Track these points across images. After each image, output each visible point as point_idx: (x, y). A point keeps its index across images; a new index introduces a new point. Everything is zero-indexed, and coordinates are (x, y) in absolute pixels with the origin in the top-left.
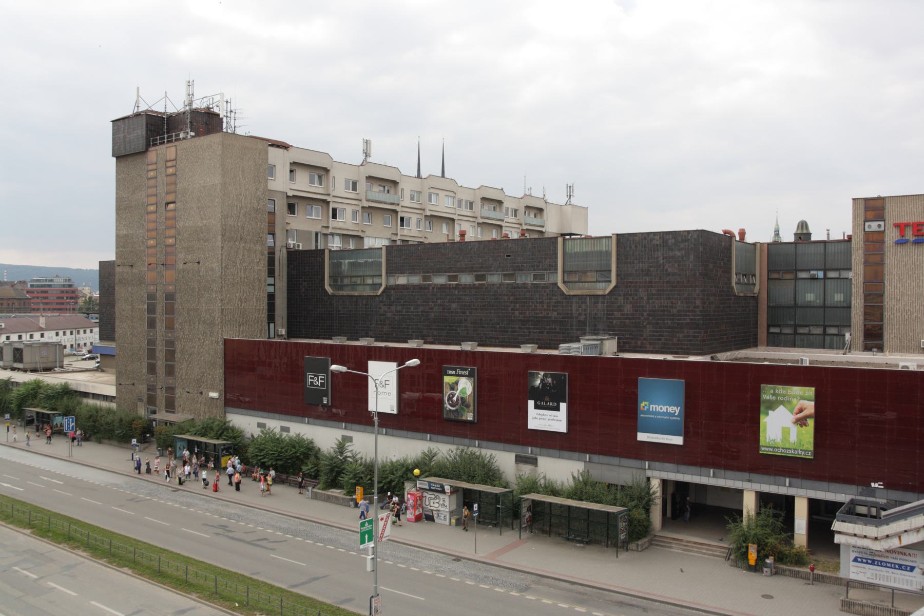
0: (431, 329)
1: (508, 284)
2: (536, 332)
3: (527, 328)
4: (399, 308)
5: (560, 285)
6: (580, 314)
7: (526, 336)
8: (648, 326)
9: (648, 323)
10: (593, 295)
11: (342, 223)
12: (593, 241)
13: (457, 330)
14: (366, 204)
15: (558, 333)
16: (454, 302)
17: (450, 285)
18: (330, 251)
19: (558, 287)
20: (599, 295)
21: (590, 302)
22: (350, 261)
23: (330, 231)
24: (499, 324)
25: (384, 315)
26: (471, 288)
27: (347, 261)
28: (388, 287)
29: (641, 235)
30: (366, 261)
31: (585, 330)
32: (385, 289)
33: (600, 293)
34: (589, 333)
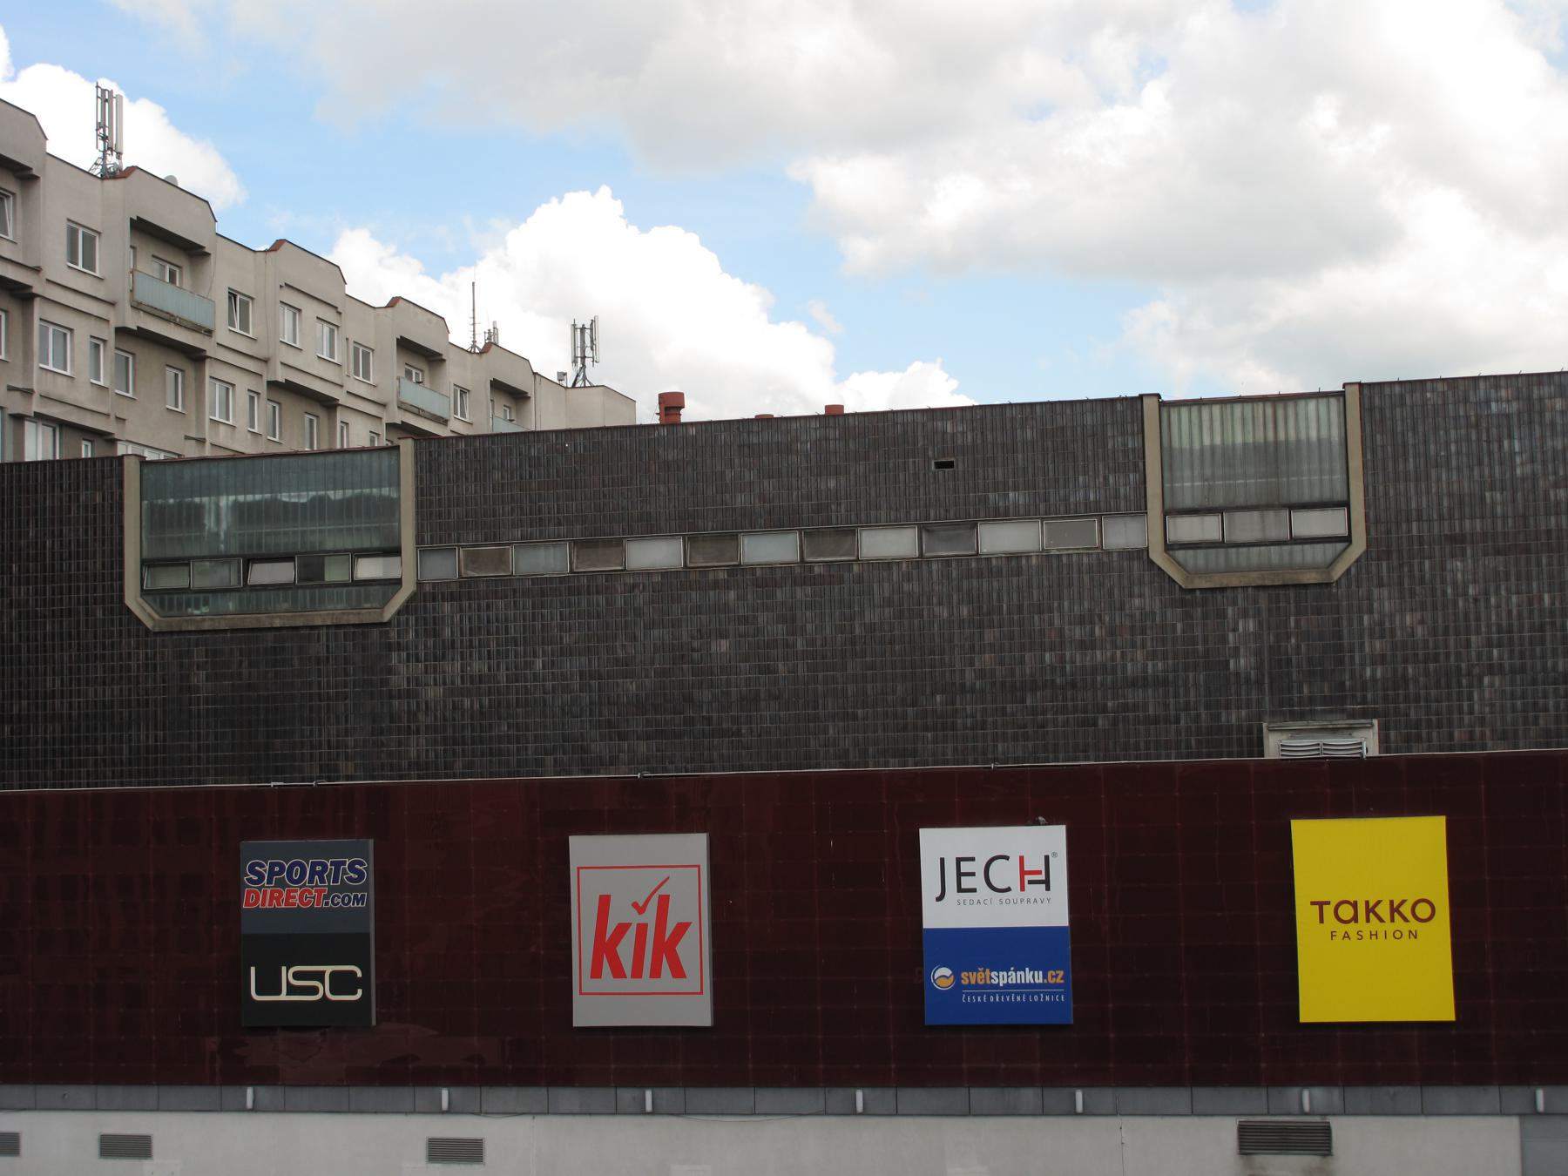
0: (622, 737)
1: (947, 562)
2: (1066, 724)
3: (1034, 711)
4: (478, 666)
5: (1158, 556)
6: (1236, 652)
7: (1026, 737)
8: (1486, 680)
9: (1490, 670)
10: (1285, 587)
11: (65, 379)
12: (1269, 411)
13: (738, 733)
14: (133, 321)
15: (1156, 721)
16: (722, 635)
17: (704, 571)
18: (143, 462)
19: (1151, 563)
20: (1306, 586)
21: (1270, 610)
22: (241, 498)
23: (36, 406)
24: (914, 704)
25: (409, 694)
26: (795, 583)
27: (225, 501)
28: (428, 589)
29: (1397, 389)
30: (322, 499)
31: (1259, 703)
32: (412, 598)
33: (1311, 577)
34: (1273, 714)
